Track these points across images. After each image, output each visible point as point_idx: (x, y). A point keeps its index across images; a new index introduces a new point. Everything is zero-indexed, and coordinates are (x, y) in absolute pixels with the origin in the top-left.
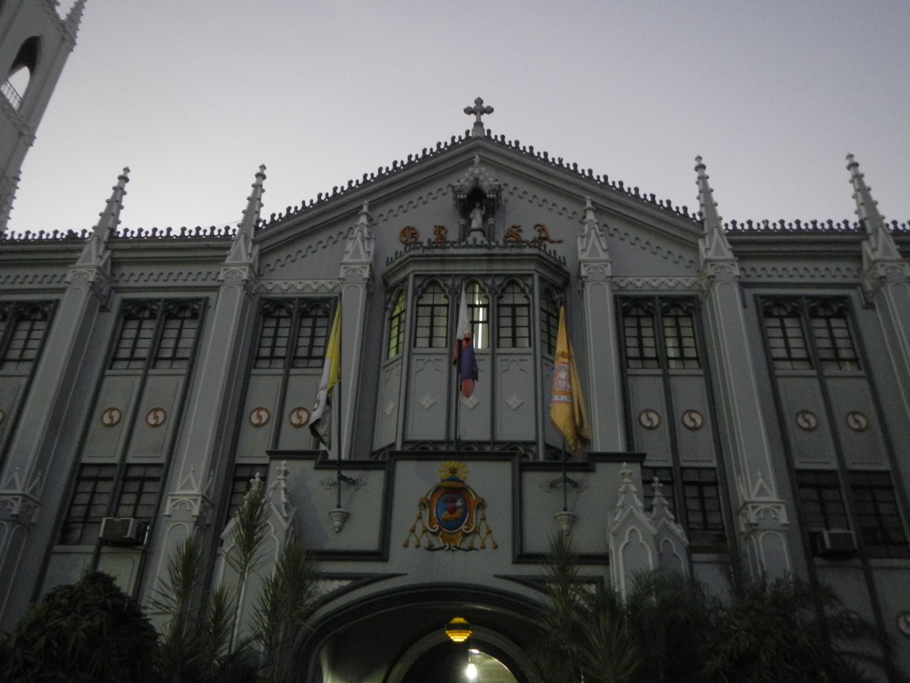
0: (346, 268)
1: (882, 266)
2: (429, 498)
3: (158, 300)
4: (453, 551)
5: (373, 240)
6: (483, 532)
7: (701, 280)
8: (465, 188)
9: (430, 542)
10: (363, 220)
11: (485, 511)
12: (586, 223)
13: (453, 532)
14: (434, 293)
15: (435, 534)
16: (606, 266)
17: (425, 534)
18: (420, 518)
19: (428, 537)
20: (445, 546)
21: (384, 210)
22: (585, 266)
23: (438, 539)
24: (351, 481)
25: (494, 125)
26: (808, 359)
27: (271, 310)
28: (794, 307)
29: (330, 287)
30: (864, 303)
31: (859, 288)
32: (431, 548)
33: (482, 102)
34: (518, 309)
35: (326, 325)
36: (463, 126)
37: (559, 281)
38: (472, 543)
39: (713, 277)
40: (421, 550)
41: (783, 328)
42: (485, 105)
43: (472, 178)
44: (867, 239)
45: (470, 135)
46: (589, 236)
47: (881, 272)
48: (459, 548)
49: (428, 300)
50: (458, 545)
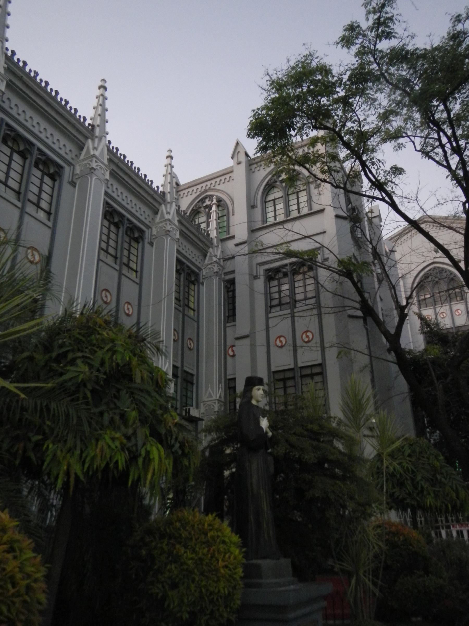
1: (96, 162)
26: (18, 193)
28: (26, 149)
30: (70, 180)
31: (72, 167)
41: (11, 158)
44: (93, 140)
47: (94, 165)
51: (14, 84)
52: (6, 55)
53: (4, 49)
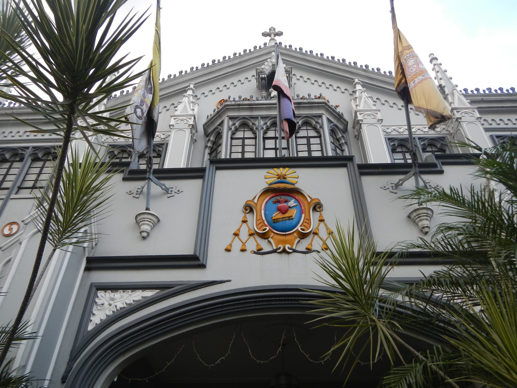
0: (175, 119)
2: (256, 201)
3: (27, 148)
4: (289, 253)
5: (197, 105)
6: (323, 232)
7: (449, 127)
8: (265, 70)
9: (258, 245)
10: (190, 92)
11: (322, 213)
12: (356, 90)
13: (287, 233)
14: (244, 131)
15: (264, 236)
16: (377, 114)
17: (252, 237)
18: (244, 222)
19: (256, 242)
20: (280, 248)
21: (206, 90)
22: (360, 114)
23: (269, 242)
24: (163, 187)
25: (284, 41)
27: (116, 153)
29: (163, 137)
32: (259, 252)
33: (274, 29)
34: (311, 140)
35: (159, 162)
36: (261, 41)
37: (341, 127)
38: (311, 244)
39: (460, 118)
40: (248, 254)
42: (277, 31)
43: (270, 64)
45: (267, 45)
46: (361, 98)
48: (295, 251)
49: (240, 134)
50: (294, 248)
51: (481, 108)
52: (463, 94)
53: (459, 92)
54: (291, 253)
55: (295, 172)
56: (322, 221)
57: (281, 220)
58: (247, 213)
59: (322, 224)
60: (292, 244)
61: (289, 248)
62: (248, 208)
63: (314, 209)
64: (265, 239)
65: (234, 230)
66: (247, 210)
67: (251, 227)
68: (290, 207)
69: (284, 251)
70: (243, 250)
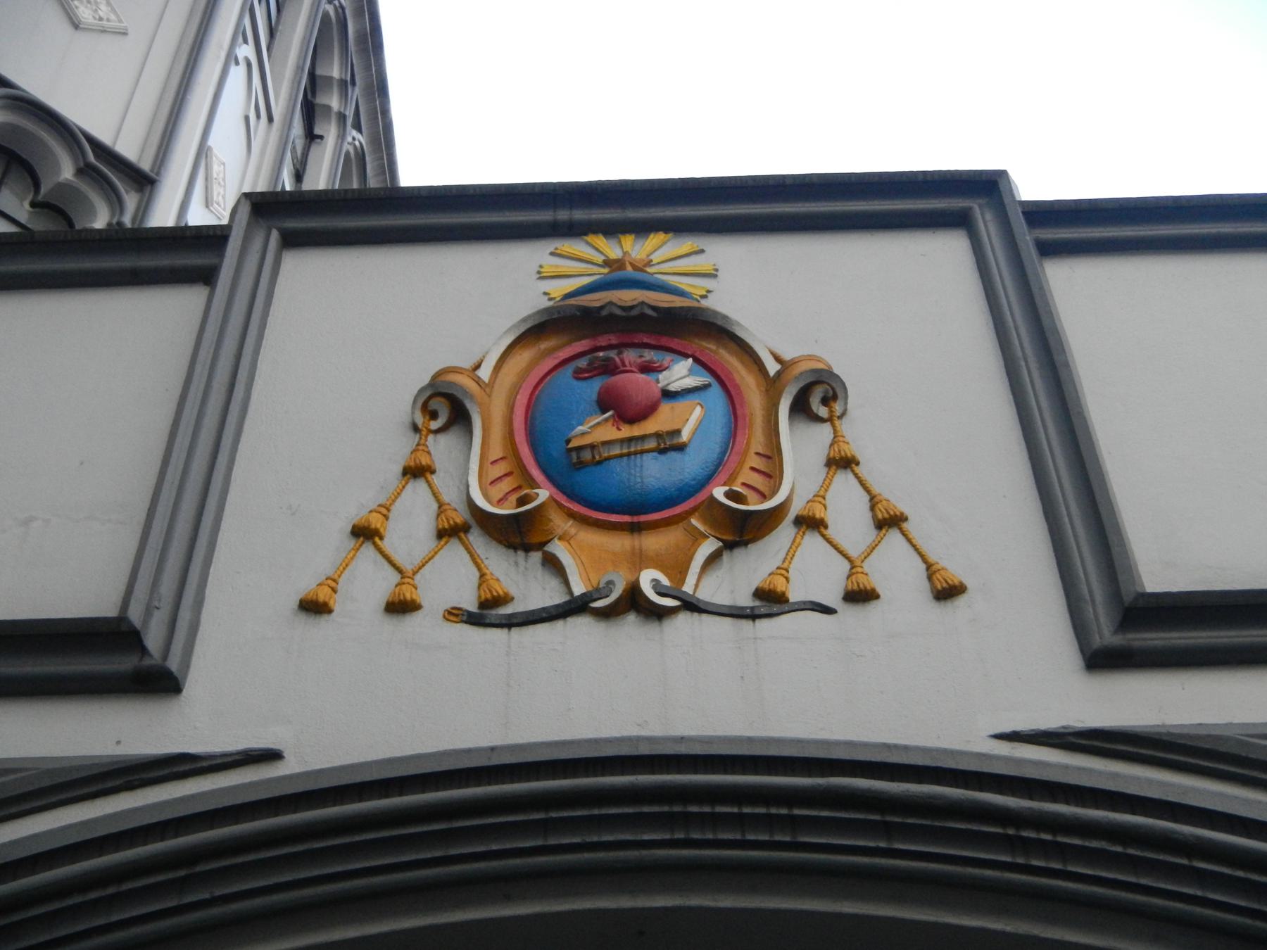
2: (485, 373)
4: (657, 614)
18: (416, 472)
38: (783, 571)
48: (691, 606)
50: (688, 587)
54: (671, 611)
55: (702, 251)
56: (842, 462)
57: (616, 451)
58: (437, 431)
59: (843, 480)
60: (678, 570)
61: (656, 585)
62: (437, 404)
63: (801, 408)
64: (527, 549)
65: (354, 510)
66: (434, 415)
67: (451, 495)
68: (668, 395)
69: (633, 602)
70: (400, 607)
